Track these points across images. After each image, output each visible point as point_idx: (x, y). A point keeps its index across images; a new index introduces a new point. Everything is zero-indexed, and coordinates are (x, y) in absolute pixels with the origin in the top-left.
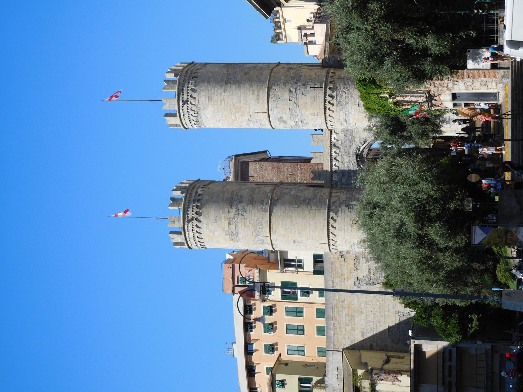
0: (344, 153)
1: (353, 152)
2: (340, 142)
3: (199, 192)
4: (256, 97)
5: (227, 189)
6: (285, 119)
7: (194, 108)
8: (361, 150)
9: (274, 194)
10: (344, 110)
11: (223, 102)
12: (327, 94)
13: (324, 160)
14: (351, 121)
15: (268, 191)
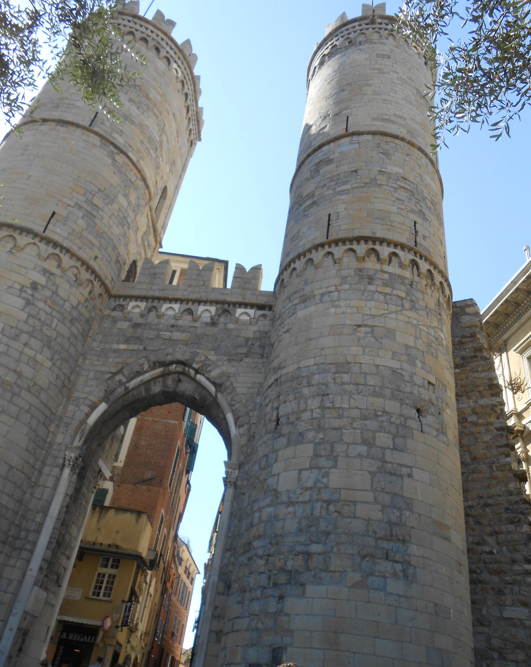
0: (199, 331)
1: (197, 354)
2: (231, 326)
3: (175, 66)
4: (387, 117)
5: (168, 113)
6: (326, 169)
7: (362, 38)
8: (199, 377)
9: (130, 163)
10: (347, 287)
11: (377, 71)
12: (398, 251)
13: (190, 286)
14: (301, 314)
15: (141, 162)
